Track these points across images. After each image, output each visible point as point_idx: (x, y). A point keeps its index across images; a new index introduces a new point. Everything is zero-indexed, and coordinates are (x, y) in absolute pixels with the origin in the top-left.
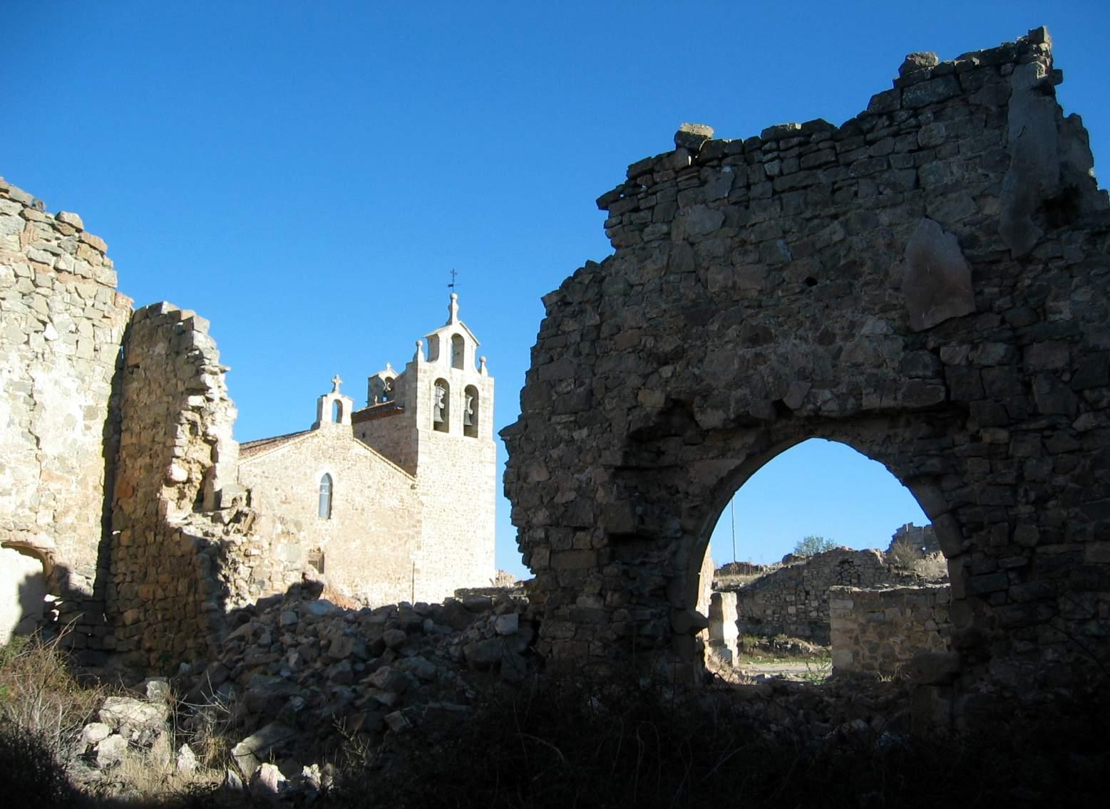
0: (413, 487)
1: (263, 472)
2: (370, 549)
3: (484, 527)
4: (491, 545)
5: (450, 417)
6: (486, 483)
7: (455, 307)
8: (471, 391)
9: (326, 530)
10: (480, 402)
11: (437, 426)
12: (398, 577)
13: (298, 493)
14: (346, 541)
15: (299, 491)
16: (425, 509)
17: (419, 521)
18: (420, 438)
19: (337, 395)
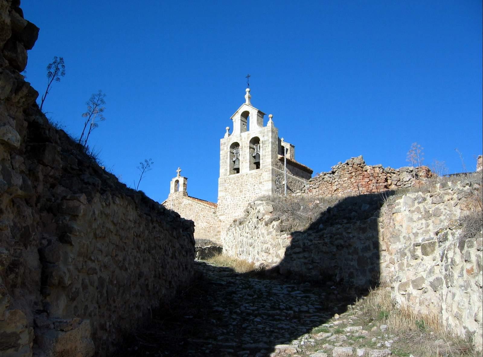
7: (247, 96)
16: (222, 224)
17: (219, 232)
18: (219, 183)
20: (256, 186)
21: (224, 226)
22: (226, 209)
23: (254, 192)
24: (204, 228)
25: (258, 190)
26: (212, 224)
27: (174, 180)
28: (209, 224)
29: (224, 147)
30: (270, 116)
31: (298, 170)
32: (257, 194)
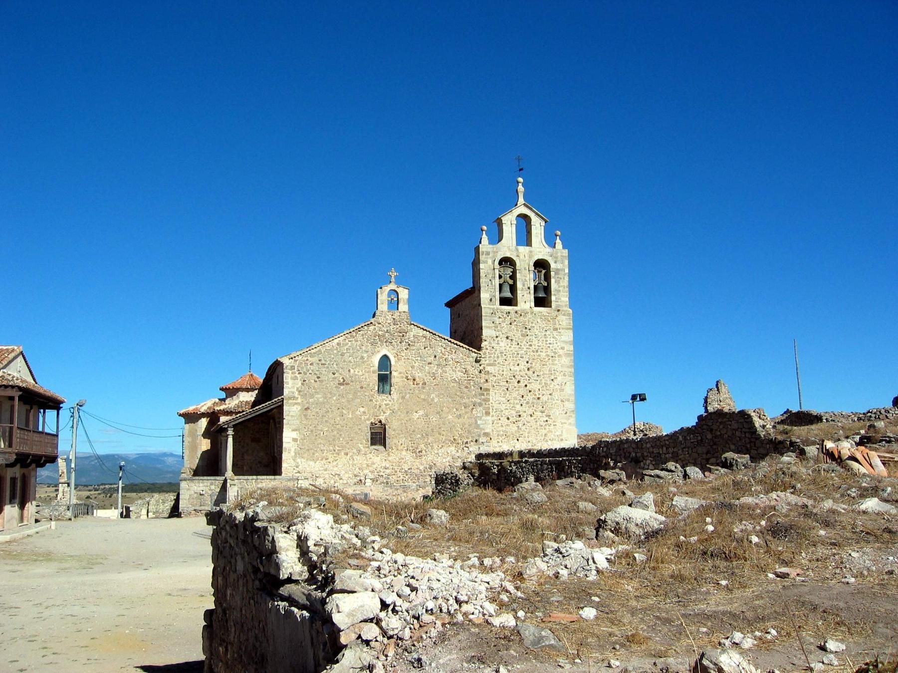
0: (477, 361)
1: (320, 360)
2: (434, 418)
3: (562, 390)
4: (570, 406)
5: (519, 292)
6: (562, 348)
7: (521, 188)
8: (541, 265)
9: (386, 405)
10: (552, 274)
11: (504, 302)
12: (465, 441)
13: (356, 375)
14: (407, 412)
15: (356, 373)
18: (483, 314)
19: (393, 286)
20: (548, 332)
21: (495, 382)
22: (498, 357)
23: (545, 339)
24: (457, 379)
25: (552, 339)
26: (472, 376)
27: (387, 289)
28: (466, 375)
29: (487, 258)
32: (550, 344)
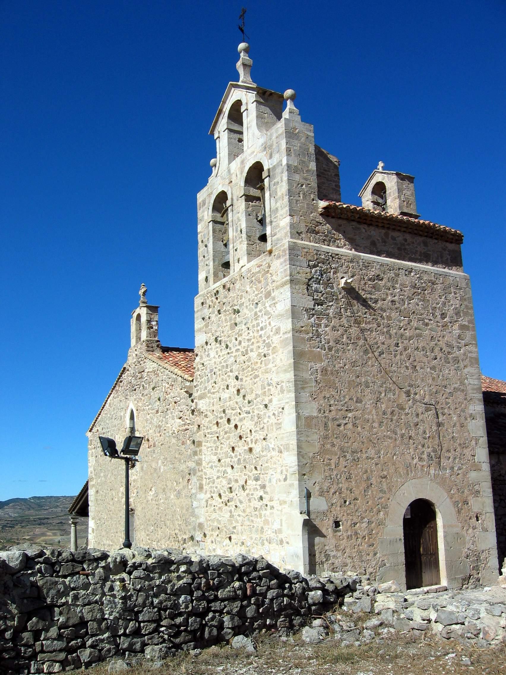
6: (278, 331)
18: (196, 310)
30: (289, 92)
31: (408, 237)
